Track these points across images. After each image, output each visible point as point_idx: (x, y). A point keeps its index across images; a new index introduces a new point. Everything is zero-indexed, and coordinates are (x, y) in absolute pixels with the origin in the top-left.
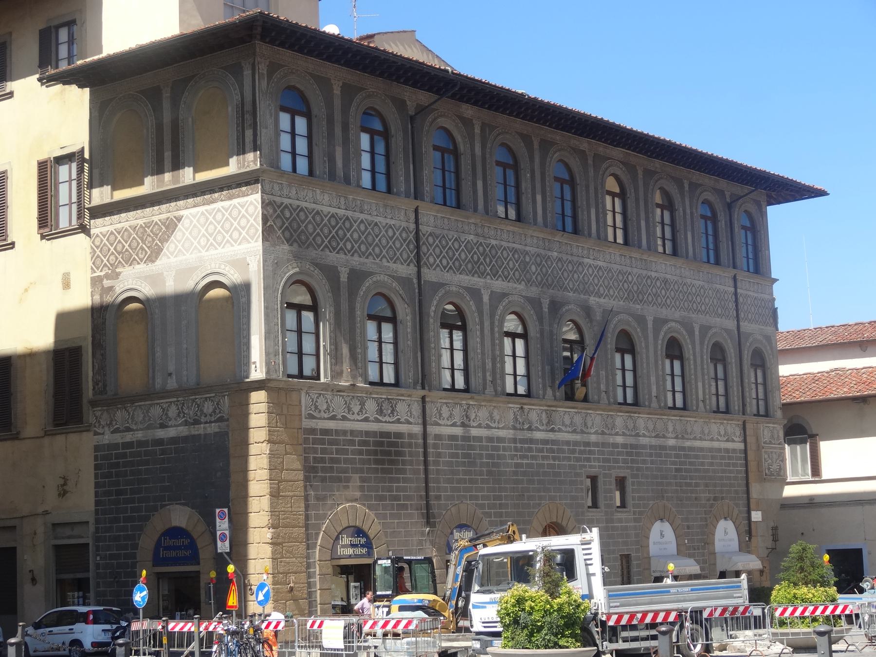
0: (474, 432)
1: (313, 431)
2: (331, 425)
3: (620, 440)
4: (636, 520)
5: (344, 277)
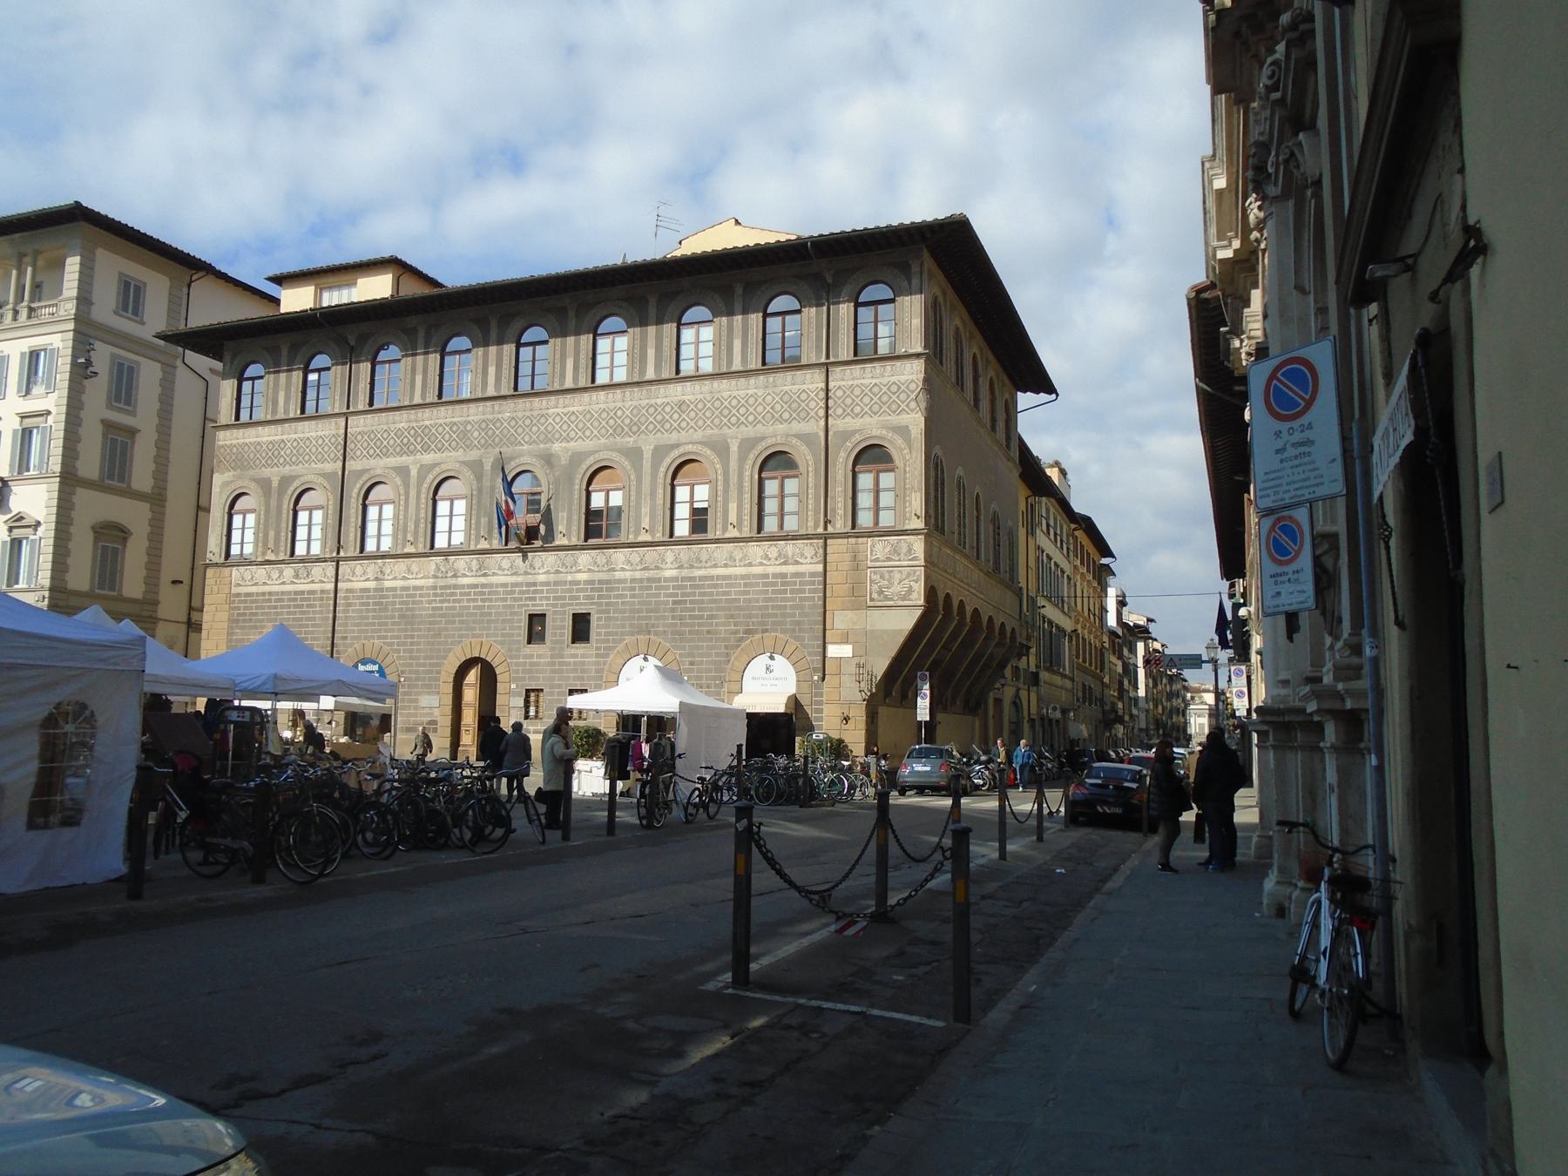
0: (387, 584)
1: (238, 595)
2: (254, 589)
3: (583, 577)
4: (597, 656)
5: (275, 484)
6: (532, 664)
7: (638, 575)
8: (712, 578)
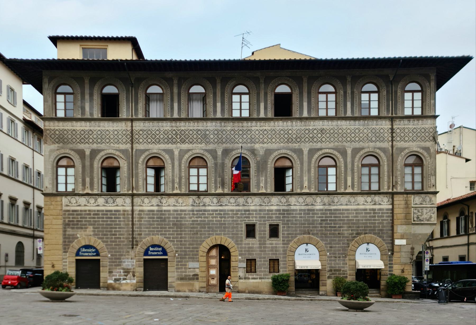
6: (249, 248)
7: (303, 208)
8: (340, 210)
